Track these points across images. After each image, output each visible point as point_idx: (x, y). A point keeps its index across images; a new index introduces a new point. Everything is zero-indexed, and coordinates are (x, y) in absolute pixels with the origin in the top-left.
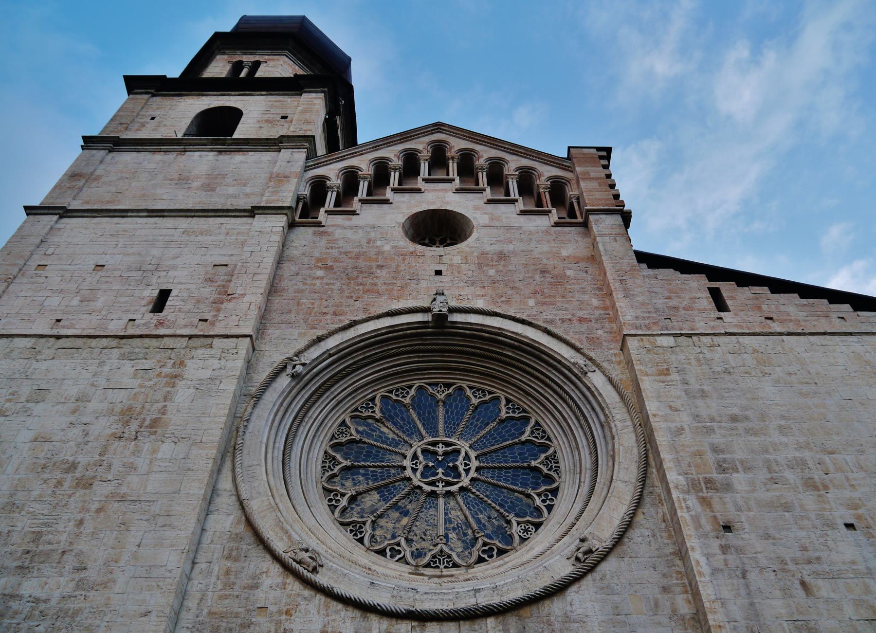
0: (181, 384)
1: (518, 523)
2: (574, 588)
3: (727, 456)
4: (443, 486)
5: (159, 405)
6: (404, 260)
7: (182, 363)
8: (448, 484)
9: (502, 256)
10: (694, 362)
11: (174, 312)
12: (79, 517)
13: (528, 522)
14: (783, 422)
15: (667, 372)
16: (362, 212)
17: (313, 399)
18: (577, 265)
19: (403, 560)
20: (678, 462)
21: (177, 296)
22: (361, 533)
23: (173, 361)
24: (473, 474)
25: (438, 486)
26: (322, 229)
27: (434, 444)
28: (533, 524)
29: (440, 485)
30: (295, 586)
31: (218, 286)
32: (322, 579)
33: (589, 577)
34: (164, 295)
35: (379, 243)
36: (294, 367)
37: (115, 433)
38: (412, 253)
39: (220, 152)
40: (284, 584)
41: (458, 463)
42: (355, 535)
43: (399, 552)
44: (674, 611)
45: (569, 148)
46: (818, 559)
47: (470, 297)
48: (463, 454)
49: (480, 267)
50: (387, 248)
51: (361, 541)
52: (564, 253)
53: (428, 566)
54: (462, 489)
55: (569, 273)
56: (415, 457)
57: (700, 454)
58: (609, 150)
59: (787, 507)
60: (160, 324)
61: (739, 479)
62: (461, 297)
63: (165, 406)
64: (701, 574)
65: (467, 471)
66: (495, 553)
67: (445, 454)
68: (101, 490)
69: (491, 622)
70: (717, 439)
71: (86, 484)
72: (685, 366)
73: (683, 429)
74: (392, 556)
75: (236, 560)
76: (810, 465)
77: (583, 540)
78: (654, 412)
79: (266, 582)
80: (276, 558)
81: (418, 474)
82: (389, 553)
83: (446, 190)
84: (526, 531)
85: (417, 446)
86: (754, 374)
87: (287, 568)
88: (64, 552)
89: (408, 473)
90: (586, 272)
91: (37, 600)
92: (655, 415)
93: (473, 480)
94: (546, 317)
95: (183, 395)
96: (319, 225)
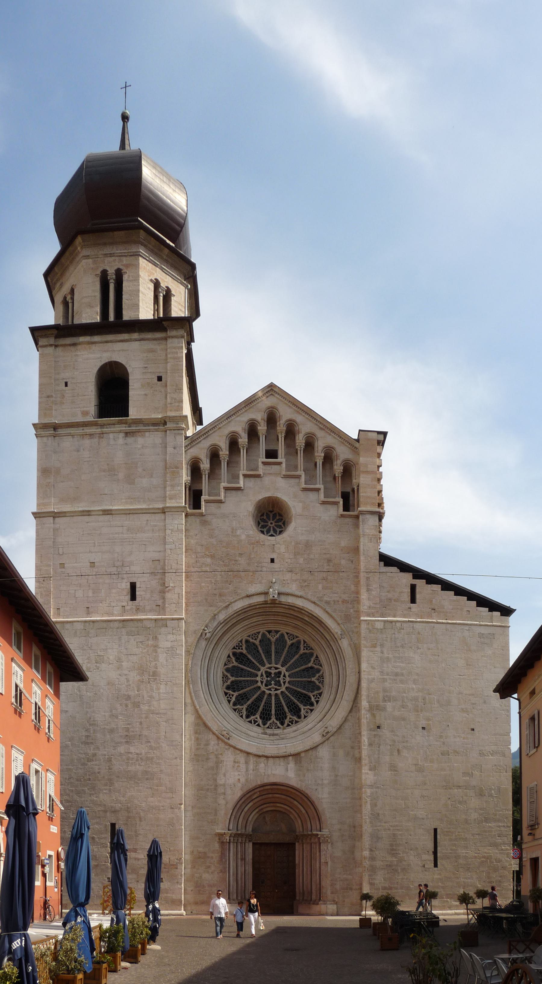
0: (159, 650)
1: (304, 709)
2: (320, 746)
3: (388, 694)
4: (274, 691)
5: (153, 664)
6: (253, 548)
7: (156, 637)
8: (276, 690)
9: (308, 545)
10: (389, 639)
11: (142, 600)
12: (139, 720)
13: (308, 708)
14: (416, 677)
15: (374, 646)
16: (227, 499)
17: (215, 648)
18: (348, 555)
19: (258, 725)
20: (368, 696)
21: (140, 587)
22: (241, 713)
23: (152, 636)
24: (287, 685)
25: (272, 691)
26: (204, 518)
27: (270, 668)
28: (310, 709)
29: (273, 690)
30: (222, 745)
31: (159, 579)
32: (230, 742)
33: (326, 742)
34: (133, 586)
35: (238, 532)
36: (206, 634)
37: (139, 680)
38: (257, 542)
39: (127, 434)
40: (219, 743)
41: (280, 679)
42: (239, 714)
43: (257, 722)
44: (353, 756)
45: (360, 431)
46: (407, 741)
47: (289, 582)
48: (283, 674)
49: (295, 555)
50: (243, 537)
51: (242, 716)
52: (343, 544)
53: (268, 728)
54: (282, 692)
55: (343, 562)
56: (262, 675)
57: (377, 692)
58: (385, 434)
59: (404, 719)
60: (138, 610)
61: (389, 706)
62: (284, 582)
63: (156, 664)
64: (364, 745)
65: (284, 683)
66: (294, 722)
67: (275, 673)
68: (145, 708)
69: (290, 758)
70: (387, 685)
71: (137, 705)
72: (385, 642)
73: (374, 679)
74: (255, 723)
75: (200, 734)
76: (420, 700)
77: (326, 728)
78: (364, 670)
79: (213, 743)
80: (214, 734)
81: (264, 684)
82: (253, 722)
83: (276, 474)
84: (307, 712)
85: (263, 669)
86: (413, 648)
87: (218, 738)
88: (140, 736)
89: (259, 684)
90: (352, 562)
91: (137, 754)
92: (364, 671)
93: (287, 688)
94: (326, 599)
95: (162, 658)
96: (202, 515)
